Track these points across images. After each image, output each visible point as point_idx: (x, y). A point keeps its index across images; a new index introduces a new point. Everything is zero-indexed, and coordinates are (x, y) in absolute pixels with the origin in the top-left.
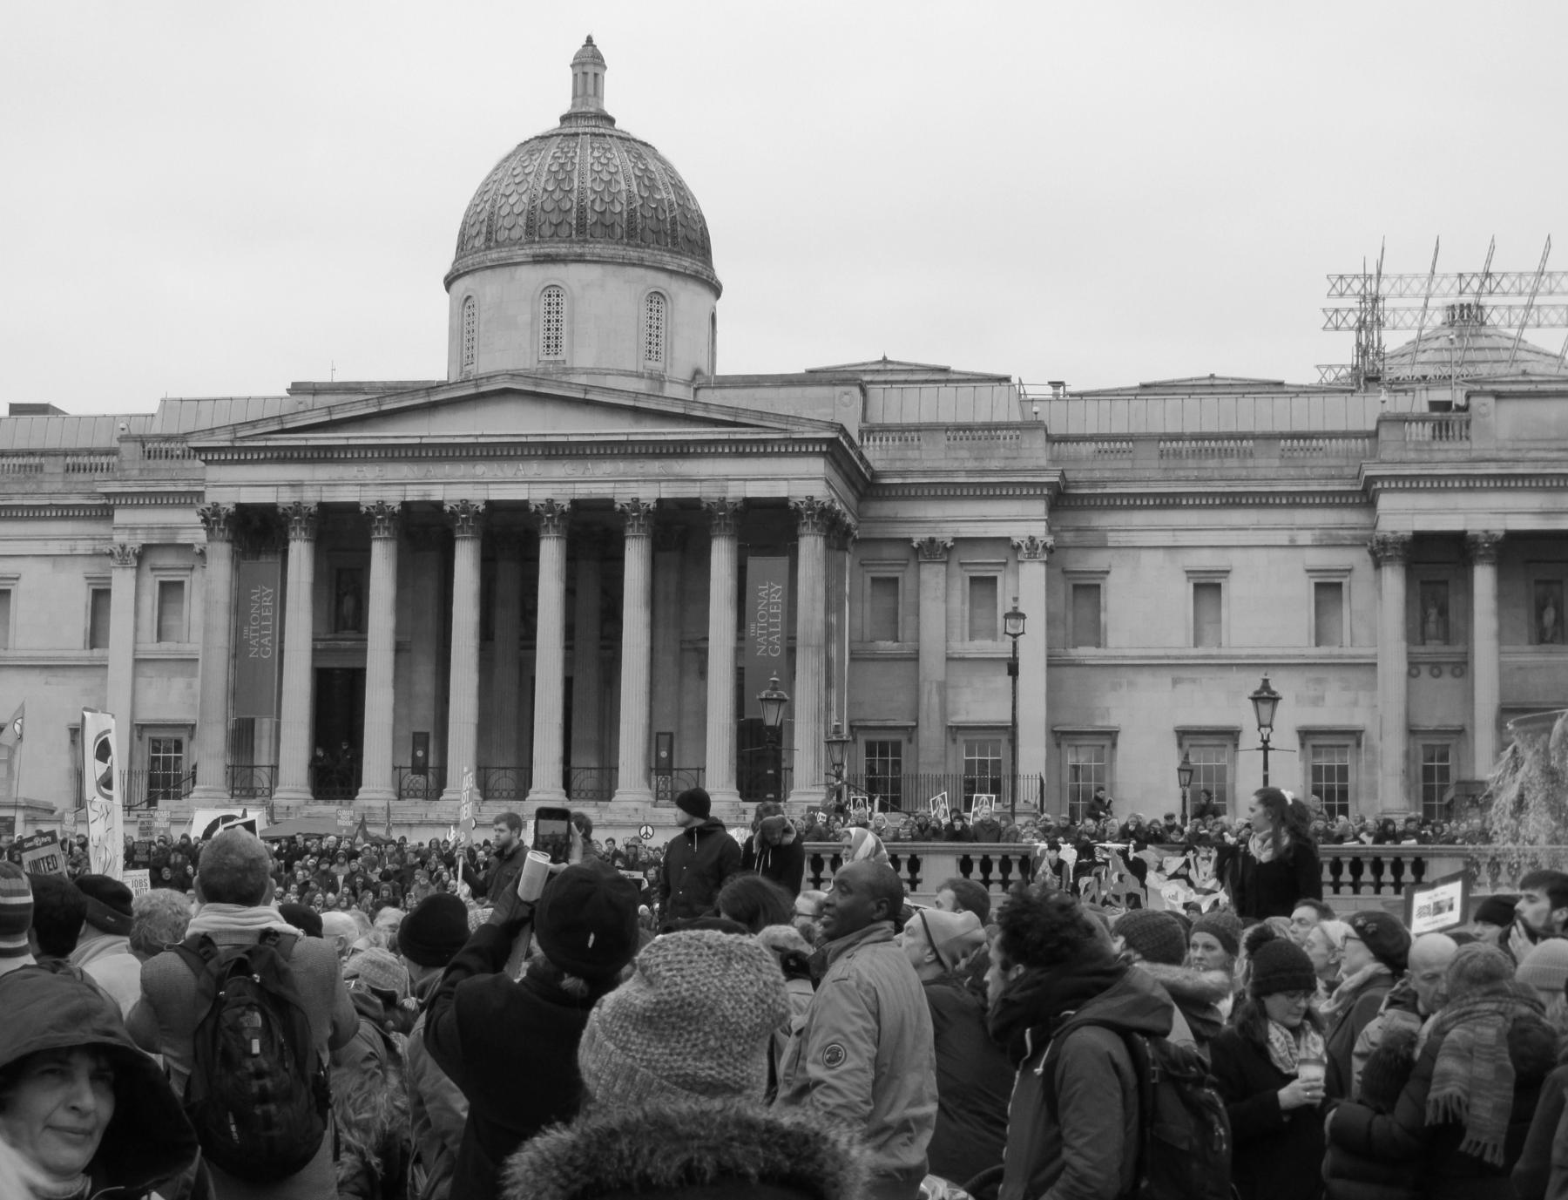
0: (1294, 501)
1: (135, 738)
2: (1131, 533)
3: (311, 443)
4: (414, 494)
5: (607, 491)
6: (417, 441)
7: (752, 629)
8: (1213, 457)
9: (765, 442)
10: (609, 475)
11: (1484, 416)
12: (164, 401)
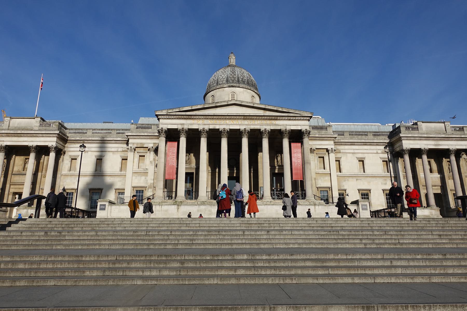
0: (378, 144)
1: (132, 190)
2: (345, 150)
3: (187, 114)
4: (212, 127)
5: (258, 127)
6: (213, 114)
10: (259, 124)
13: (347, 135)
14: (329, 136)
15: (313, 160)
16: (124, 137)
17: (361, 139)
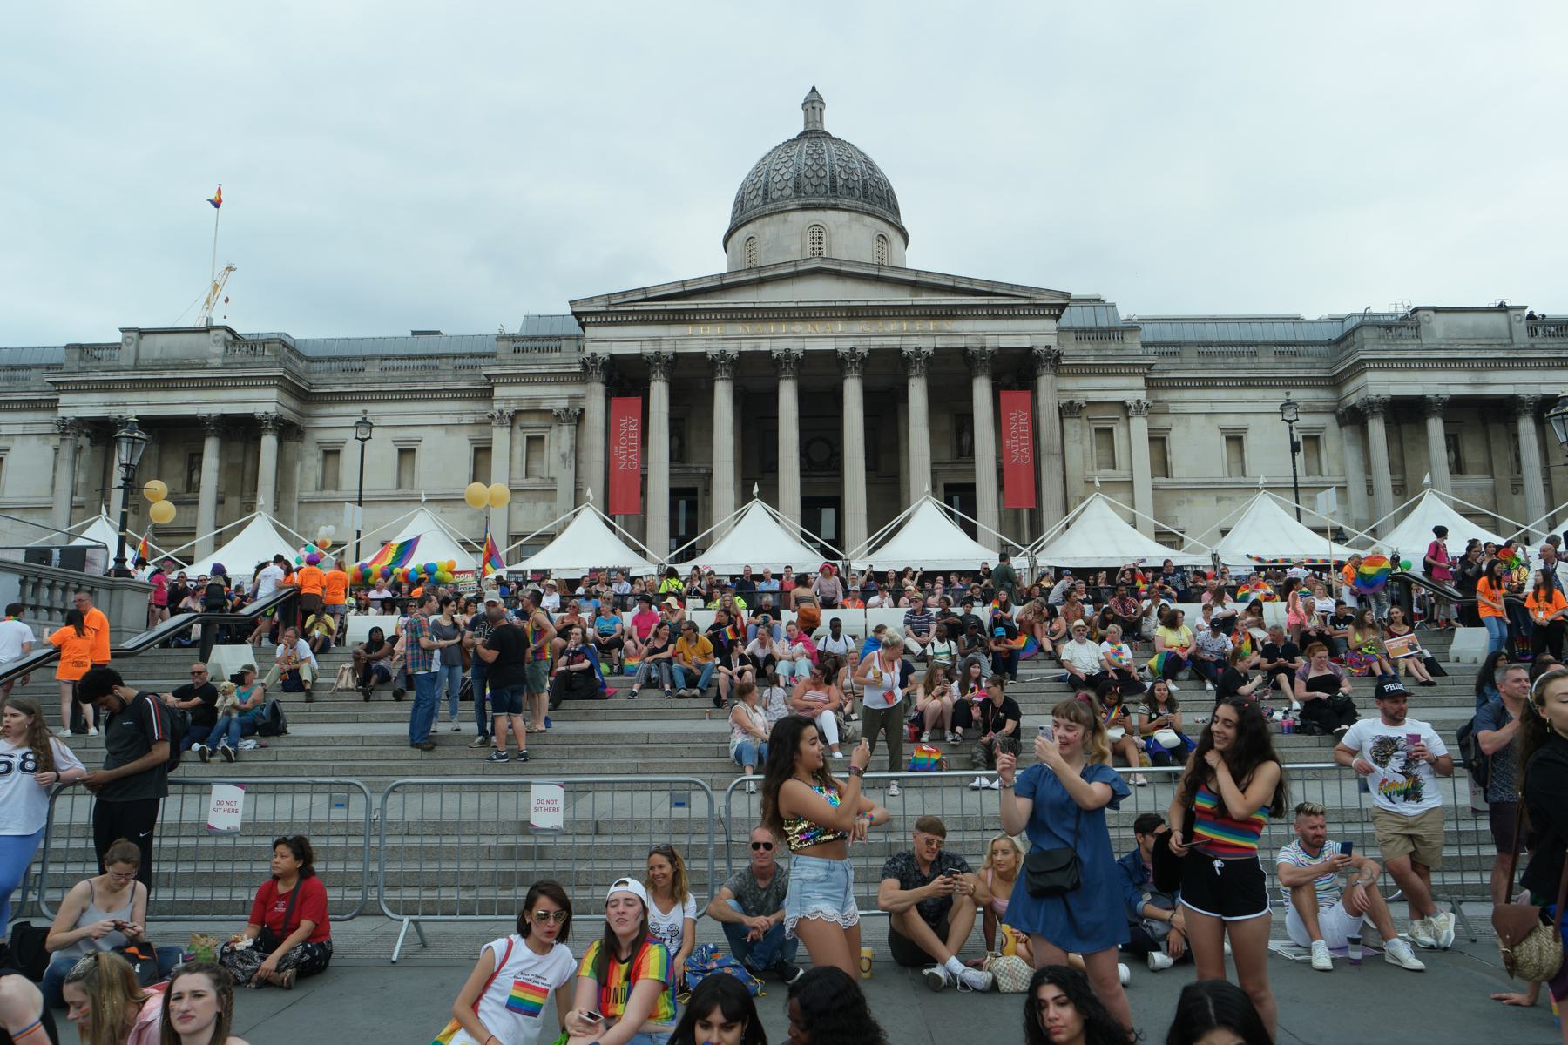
0: (1289, 383)
3: (668, 308)
4: (747, 346)
6: (752, 305)
7: (1007, 443)
8: (1232, 356)
9: (1013, 306)
10: (894, 331)
11: (1428, 323)
12: (527, 317)
13: (1190, 355)
14: (1131, 362)
15: (1077, 438)
16: (477, 378)
17: (1235, 367)
